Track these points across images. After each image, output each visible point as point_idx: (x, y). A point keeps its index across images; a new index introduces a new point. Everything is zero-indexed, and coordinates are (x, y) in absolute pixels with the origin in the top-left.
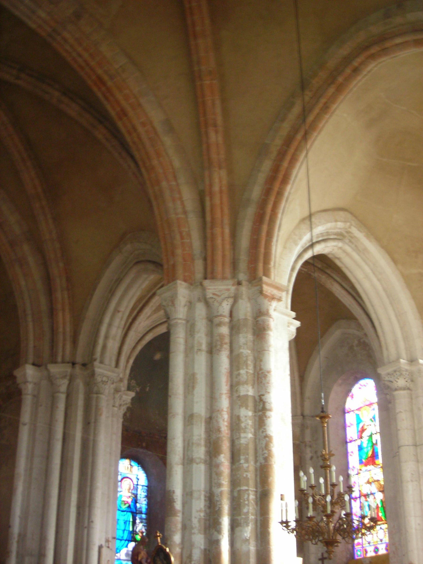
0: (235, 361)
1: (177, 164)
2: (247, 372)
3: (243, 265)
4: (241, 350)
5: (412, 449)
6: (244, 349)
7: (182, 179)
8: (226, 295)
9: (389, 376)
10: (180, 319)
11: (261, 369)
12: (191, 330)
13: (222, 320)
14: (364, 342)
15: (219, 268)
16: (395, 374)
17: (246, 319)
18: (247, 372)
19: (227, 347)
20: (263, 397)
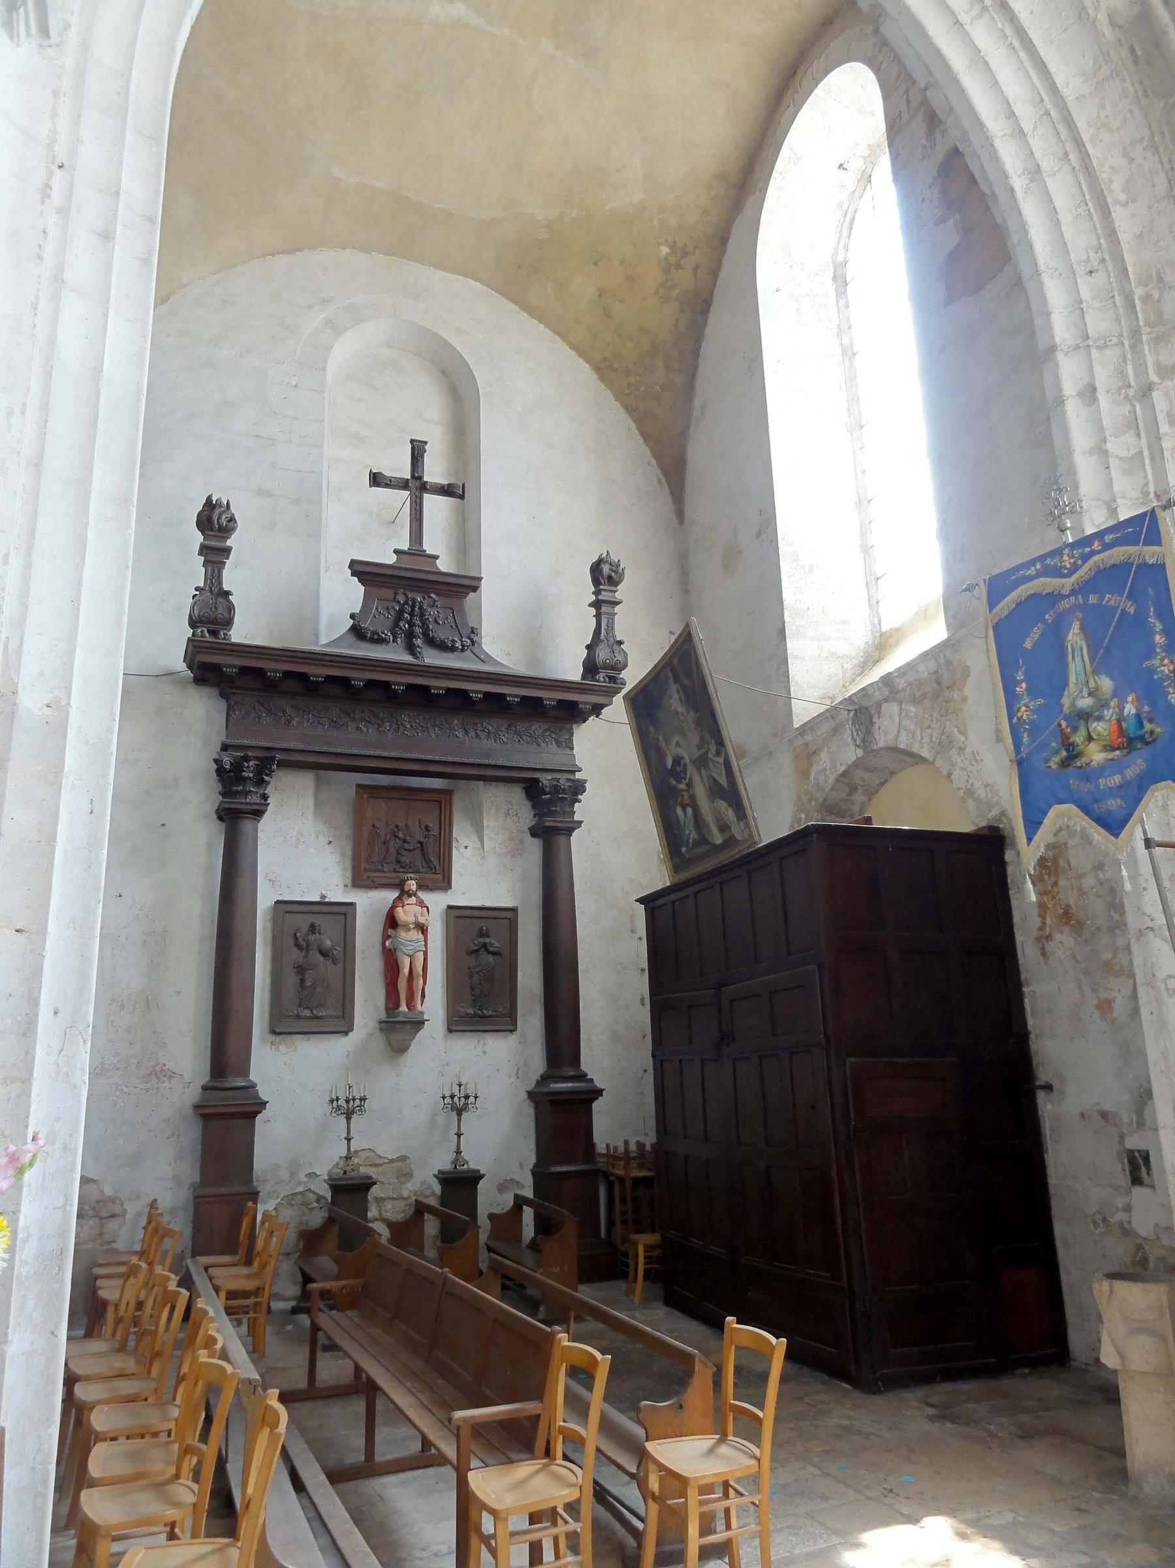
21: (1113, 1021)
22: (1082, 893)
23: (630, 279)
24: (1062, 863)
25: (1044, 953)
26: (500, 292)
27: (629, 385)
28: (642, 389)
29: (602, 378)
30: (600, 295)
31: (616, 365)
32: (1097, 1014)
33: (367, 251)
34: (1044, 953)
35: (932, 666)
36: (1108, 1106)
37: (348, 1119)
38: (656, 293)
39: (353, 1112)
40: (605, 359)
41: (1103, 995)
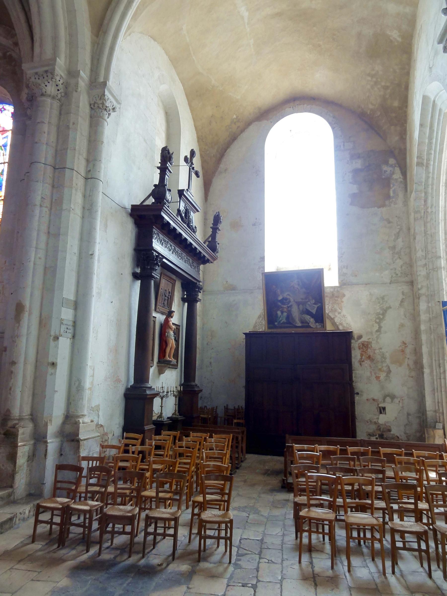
5: (49, 170)
9: (37, 77)
14: (10, 56)
16: (45, 75)
21: (380, 381)
22: (374, 353)
23: (222, 117)
24: (369, 346)
26: (186, 95)
27: (205, 149)
28: (208, 152)
29: (198, 141)
30: (212, 116)
31: (204, 140)
32: (375, 379)
33: (167, 55)
34: (361, 364)
35: (332, 290)
36: (375, 398)
37: (162, 399)
38: (226, 127)
39: (164, 397)
40: (202, 136)
41: (377, 375)
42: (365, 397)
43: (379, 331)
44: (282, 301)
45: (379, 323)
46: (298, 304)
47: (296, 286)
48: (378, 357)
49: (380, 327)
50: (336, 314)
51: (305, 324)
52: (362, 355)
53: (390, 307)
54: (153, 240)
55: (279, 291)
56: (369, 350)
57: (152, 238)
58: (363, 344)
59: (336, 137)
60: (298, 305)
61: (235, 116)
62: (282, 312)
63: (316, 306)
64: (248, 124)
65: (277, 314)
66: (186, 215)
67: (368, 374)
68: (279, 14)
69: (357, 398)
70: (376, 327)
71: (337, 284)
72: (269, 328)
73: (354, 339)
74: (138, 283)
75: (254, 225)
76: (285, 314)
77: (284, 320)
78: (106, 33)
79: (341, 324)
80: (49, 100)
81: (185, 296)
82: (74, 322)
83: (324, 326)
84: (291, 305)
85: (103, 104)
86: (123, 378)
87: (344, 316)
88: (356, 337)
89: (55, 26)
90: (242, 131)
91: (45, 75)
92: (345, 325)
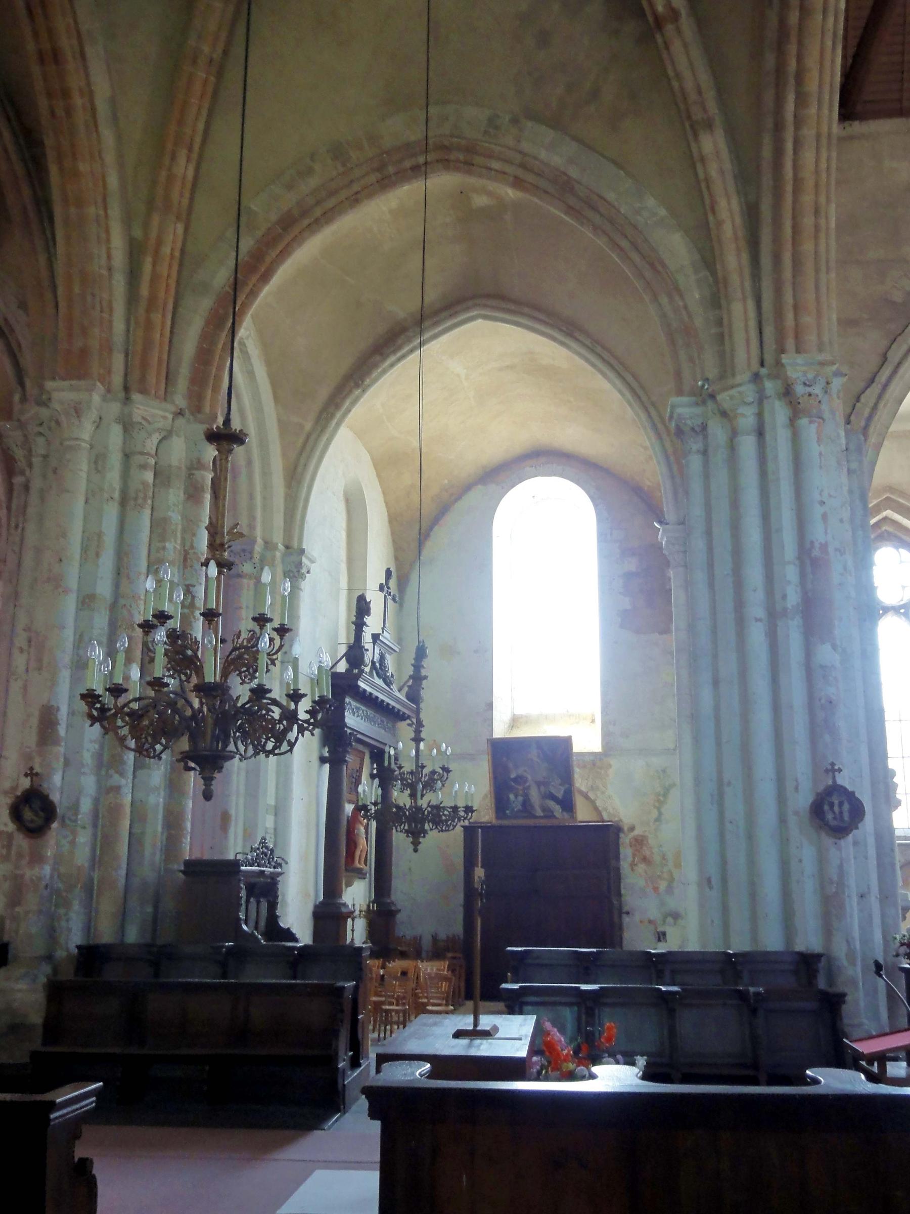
0: (159, 527)
1: (113, 181)
2: (175, 548)
3: (182, 384)
4: (170, 513)
6: (173, 511)
7: (115, 212)
8: (160, 425)
10: (84, 441)
11: (192, 547)
12: (99, 461)
13: (149, 461)
15: (152, 379)
16: (242, 554)
17: (180, 468)
18: (175, 548)
19: (149, 502)
20: (191, 588)
22: (652, 853)
25: (632, 870)
29: (390, 522)
34: (632, 870)
35: (592, 758)
36: (652, 918)
42: (637, 917)
43: (658, 820)
44: (515, 780)
45: (659, 809)
46: (539, 784)
47: (535, 759)
48: (657, 859)
49: (660, 814)
50: (599, 793)
51: (549, 814)
52: (634, 856)
53: (673, 785)
54: (346, 714)
55: (511, 765)
56: (645, 848)
57: (343, 710)
58: (636, 840)
59: (599, 520)
60: (539, 788)
61: (446, 481)
62: (516, 796)
63: (563, 789)
64: (468, 488)
65: (508, 798)
66: (381, 665)
67: (642, 883)
68: (511, 367)
69: (626, 919)
70: (655, 814)
71: (600, 750)
72: (497, 818)
73: (623, 832)
74: (327, 766)
75: (476, 651)
76: (520, 799)
77: (520, 807)
78: (300, 483)
79: (606, 809)
80: (245, 581)
81: (375, 772)
82: (275, 829)
83: (573, 817)
84: (529, 786)
85: (299, 571)
86: (312, 893)
87: (610, 797)
88: (626, 829)
89: (251, 497)
90: (459, 498)
91: (242, 554)
92: (611, 811)
